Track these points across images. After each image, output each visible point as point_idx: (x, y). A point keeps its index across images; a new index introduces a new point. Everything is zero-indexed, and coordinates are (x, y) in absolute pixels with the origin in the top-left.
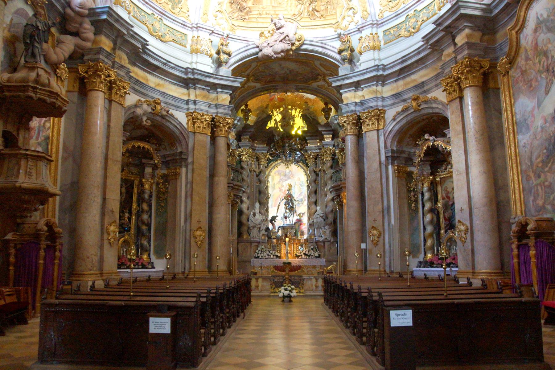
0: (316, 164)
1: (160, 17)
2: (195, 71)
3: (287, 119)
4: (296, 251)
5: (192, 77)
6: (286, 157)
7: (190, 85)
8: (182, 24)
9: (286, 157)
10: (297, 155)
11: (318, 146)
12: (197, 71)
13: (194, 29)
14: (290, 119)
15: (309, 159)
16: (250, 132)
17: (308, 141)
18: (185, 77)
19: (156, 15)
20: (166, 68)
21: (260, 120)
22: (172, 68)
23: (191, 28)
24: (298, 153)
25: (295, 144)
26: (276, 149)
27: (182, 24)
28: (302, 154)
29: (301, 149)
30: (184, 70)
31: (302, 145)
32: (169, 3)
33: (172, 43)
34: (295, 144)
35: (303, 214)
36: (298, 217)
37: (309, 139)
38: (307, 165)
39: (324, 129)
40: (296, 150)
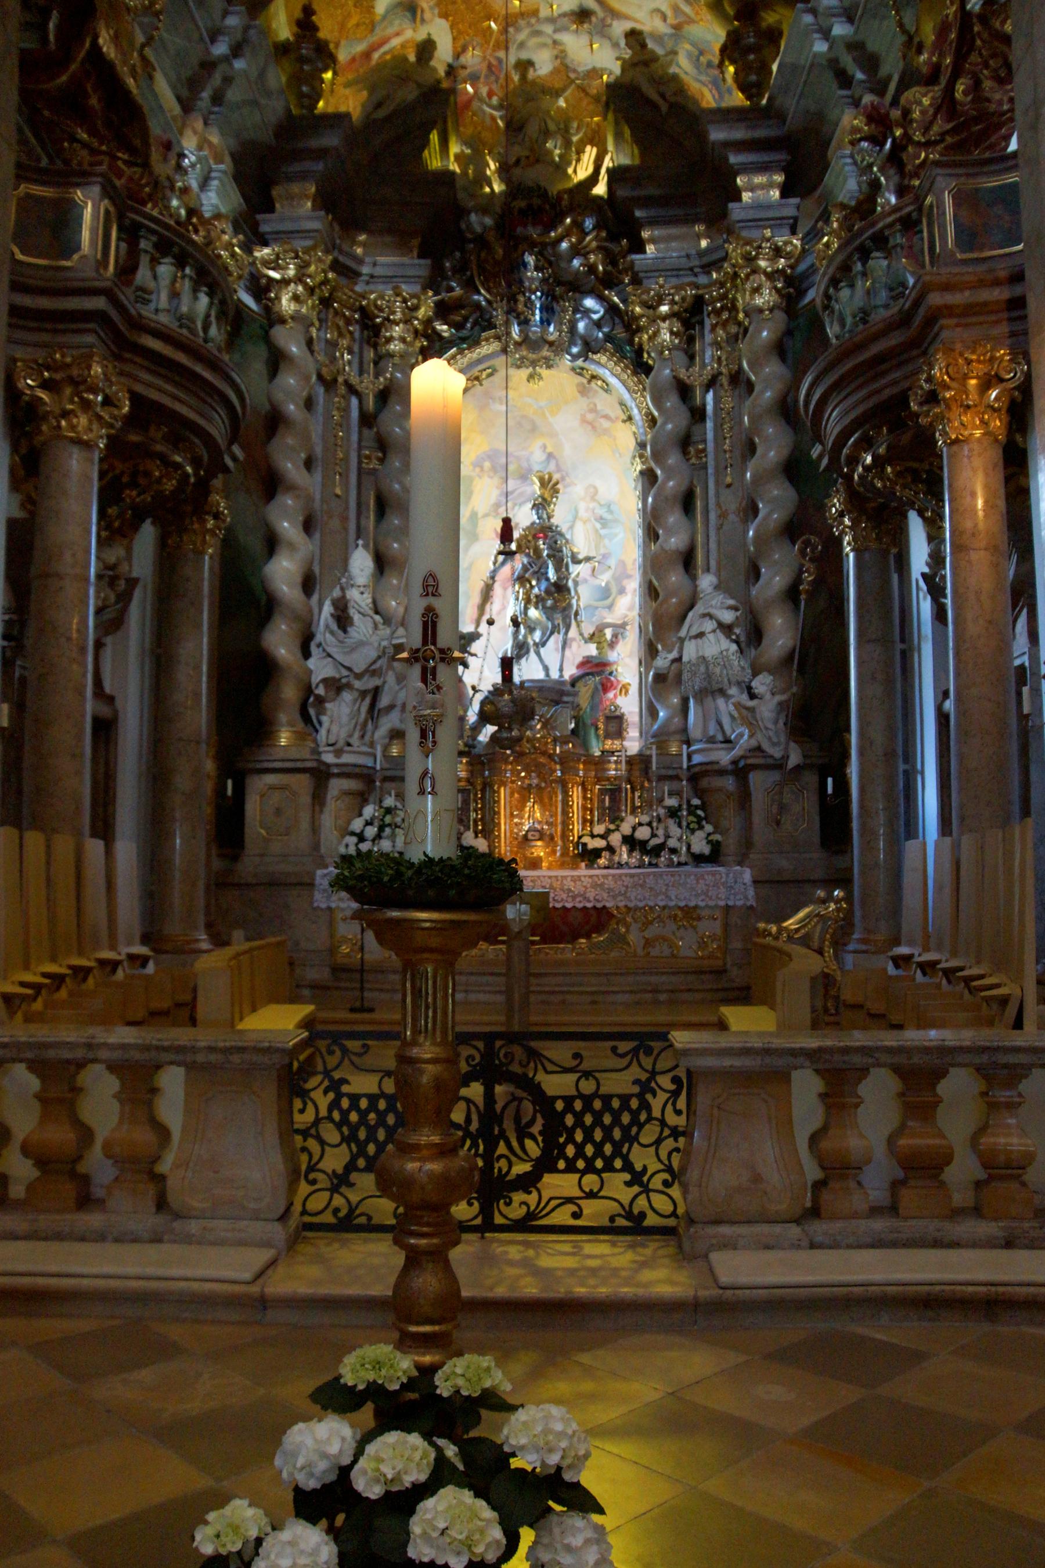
0: (692, 357)
3: (532, 130)
4: (577, 828)
6: (525, 323)
9: (525, 323)
10: (587, 312)
11: (701, 254)
14: (546, 134)
15: (653, 321)
16: (321, 153)
17: (645, 234)
21: (381, 114)
24: (589, 303)
25: (576, 251)
26: (470, 286)
28: (612, 310)
29: (609, 281)
31: (611, 259)
34: (576, 251)
35: (619, 629)
36: (592, 650)
37: (653, 223)
38: (641, 367)
39: (739, 134)
40: (577, 287)
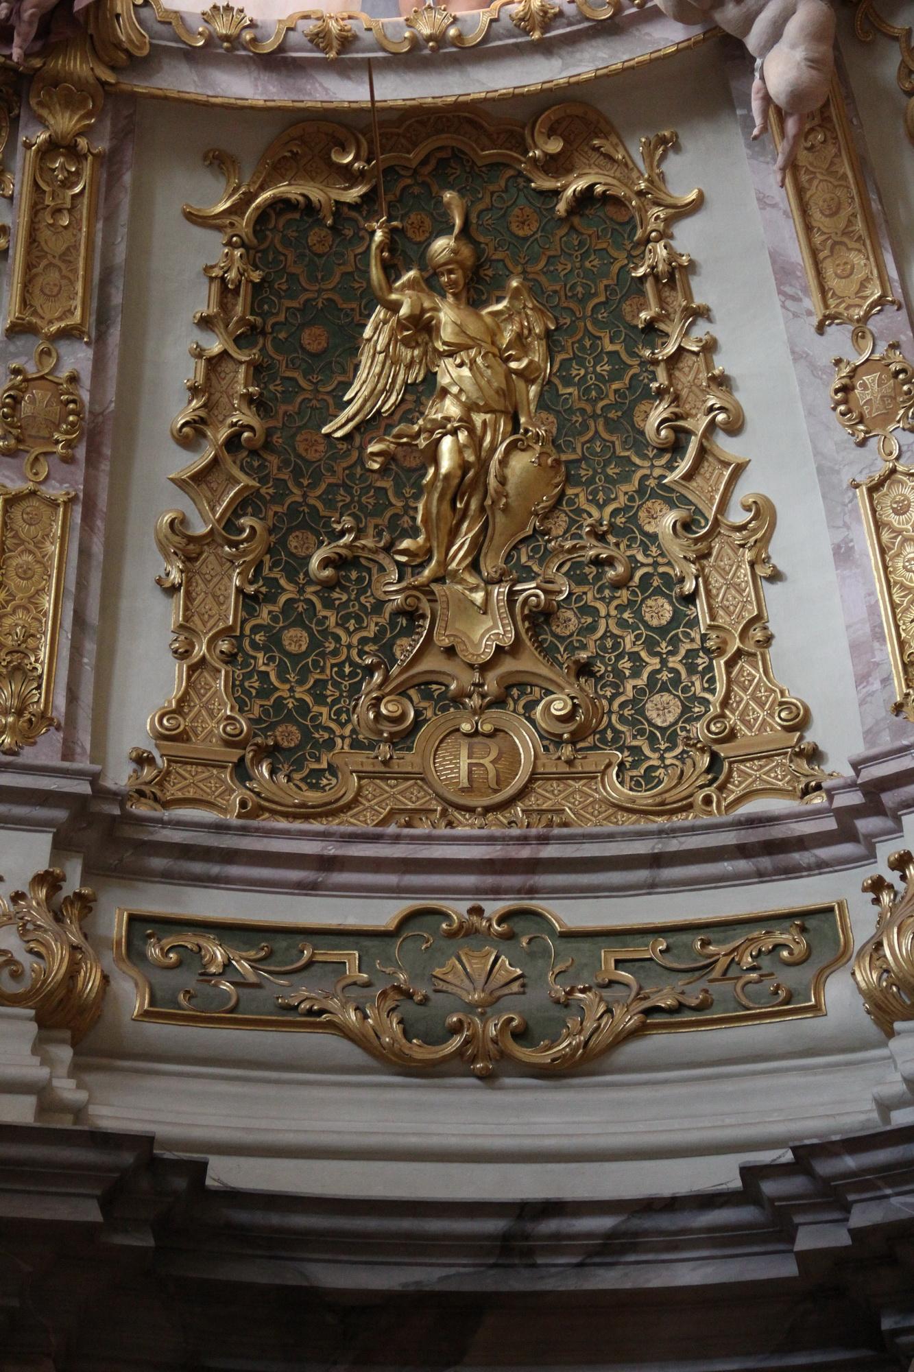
1: (494, 908)
2: (825, 1167)
5: (839, 1238)
7: (887, 1324)
8: (742, 851)
12: (850, 1162)
13: (865, 825)
18: (787, 1268)
19: (458, 908)
20: (558, 1278)
22: (610, 1248)
23: (846, 834)
27: (742, 851)
30: (745, 1214)
32: (593, 761)
33: (658, 1042)
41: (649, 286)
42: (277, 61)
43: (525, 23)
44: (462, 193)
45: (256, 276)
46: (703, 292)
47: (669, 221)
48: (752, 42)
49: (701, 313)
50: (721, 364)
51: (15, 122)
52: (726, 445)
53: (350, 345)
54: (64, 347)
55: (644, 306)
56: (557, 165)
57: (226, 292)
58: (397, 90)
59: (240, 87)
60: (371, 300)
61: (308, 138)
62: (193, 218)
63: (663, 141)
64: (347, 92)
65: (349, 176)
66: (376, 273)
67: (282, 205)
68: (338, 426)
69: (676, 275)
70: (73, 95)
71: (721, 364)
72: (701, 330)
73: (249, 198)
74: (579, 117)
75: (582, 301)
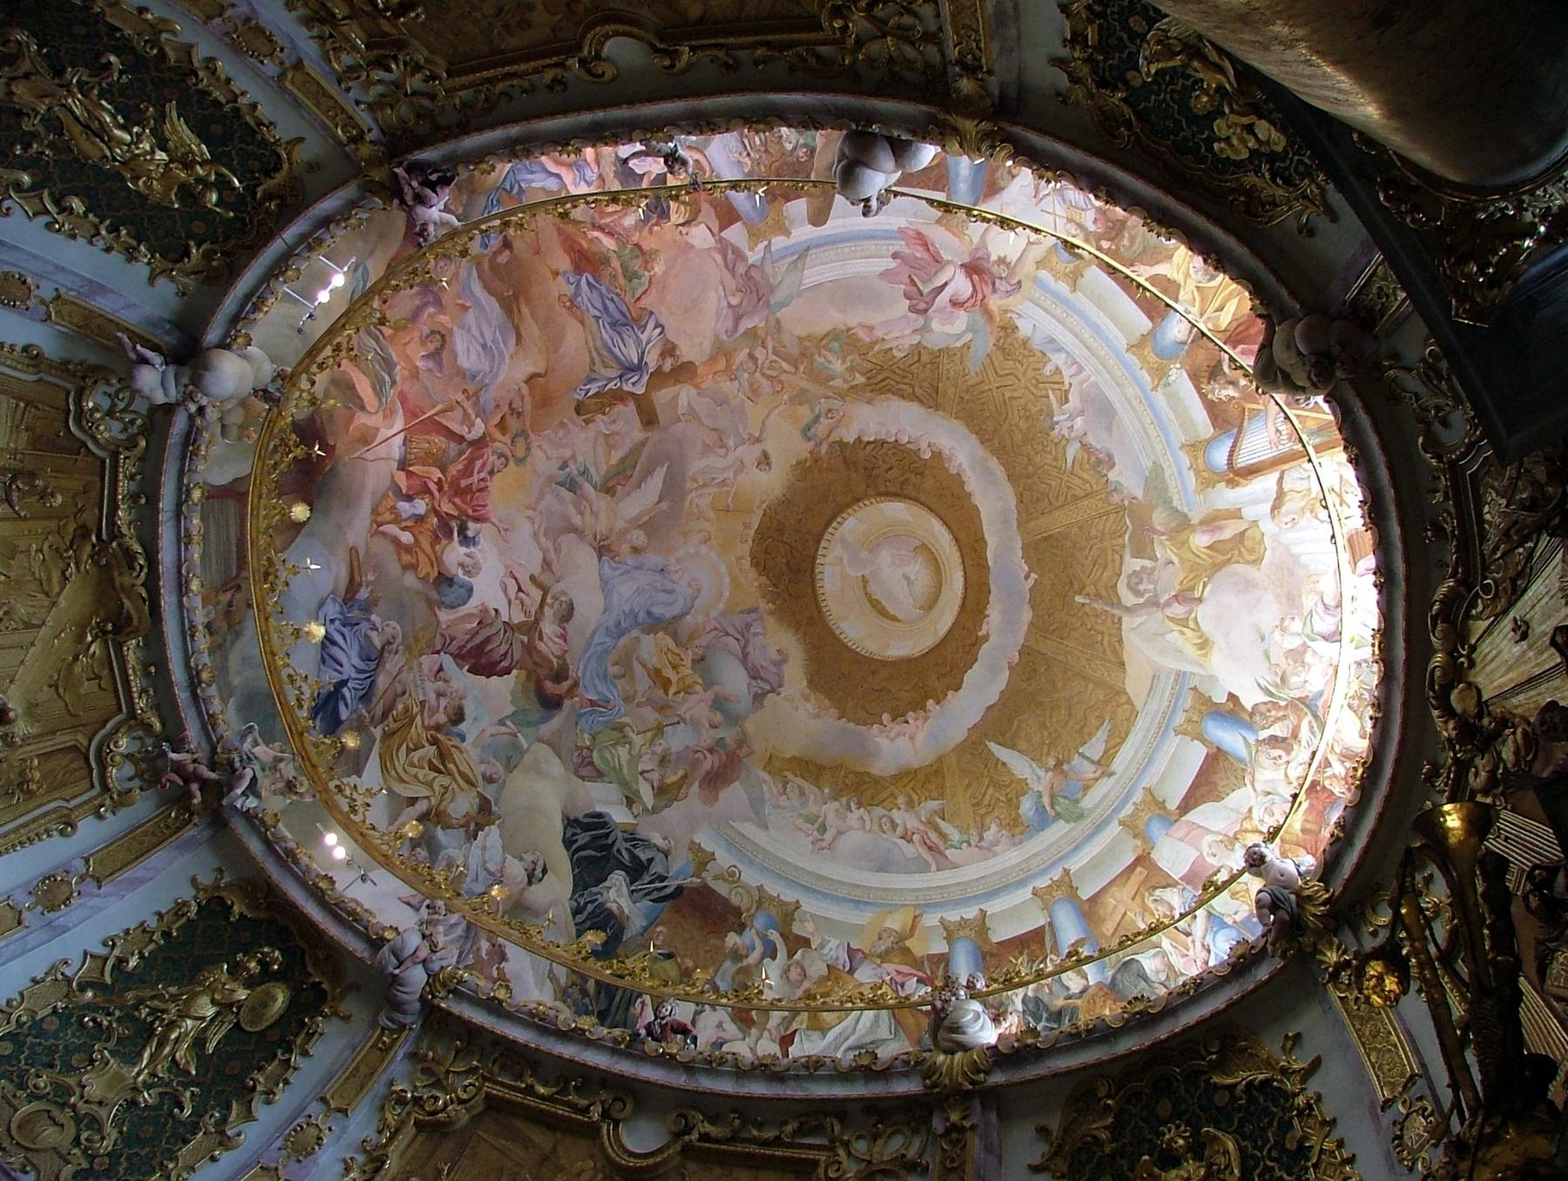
41: (134, 243)
42: (325, 222)
43: (262, 300)
44: (229, 220)
45: (259, 137)
46: (117, 257)
47: (153, 270)
48: (171, 369)
49: (108, 250)
50: (81, 241)
51: (384, 133)
52: (49, 219)
53: (204, 136)
54: (278, 70)
55: (128, 234)
56: (207, 256)
57: (260, 123)
58: (276, 247)
59: (328, 205)
60: (216, 159)
61: (293, 201)
62: (301, 140)
63: (184, 294)
64: (290, 234)
65: (269, 196)
66: (225, 170)
67: (277, 169)
68: (172, 109)
69: (131, 255)
70: (373, 162)
71: (81, 241)
72: (101, 244)
73: (291, 164)
74: (219, 277)
75: (150, 218)
